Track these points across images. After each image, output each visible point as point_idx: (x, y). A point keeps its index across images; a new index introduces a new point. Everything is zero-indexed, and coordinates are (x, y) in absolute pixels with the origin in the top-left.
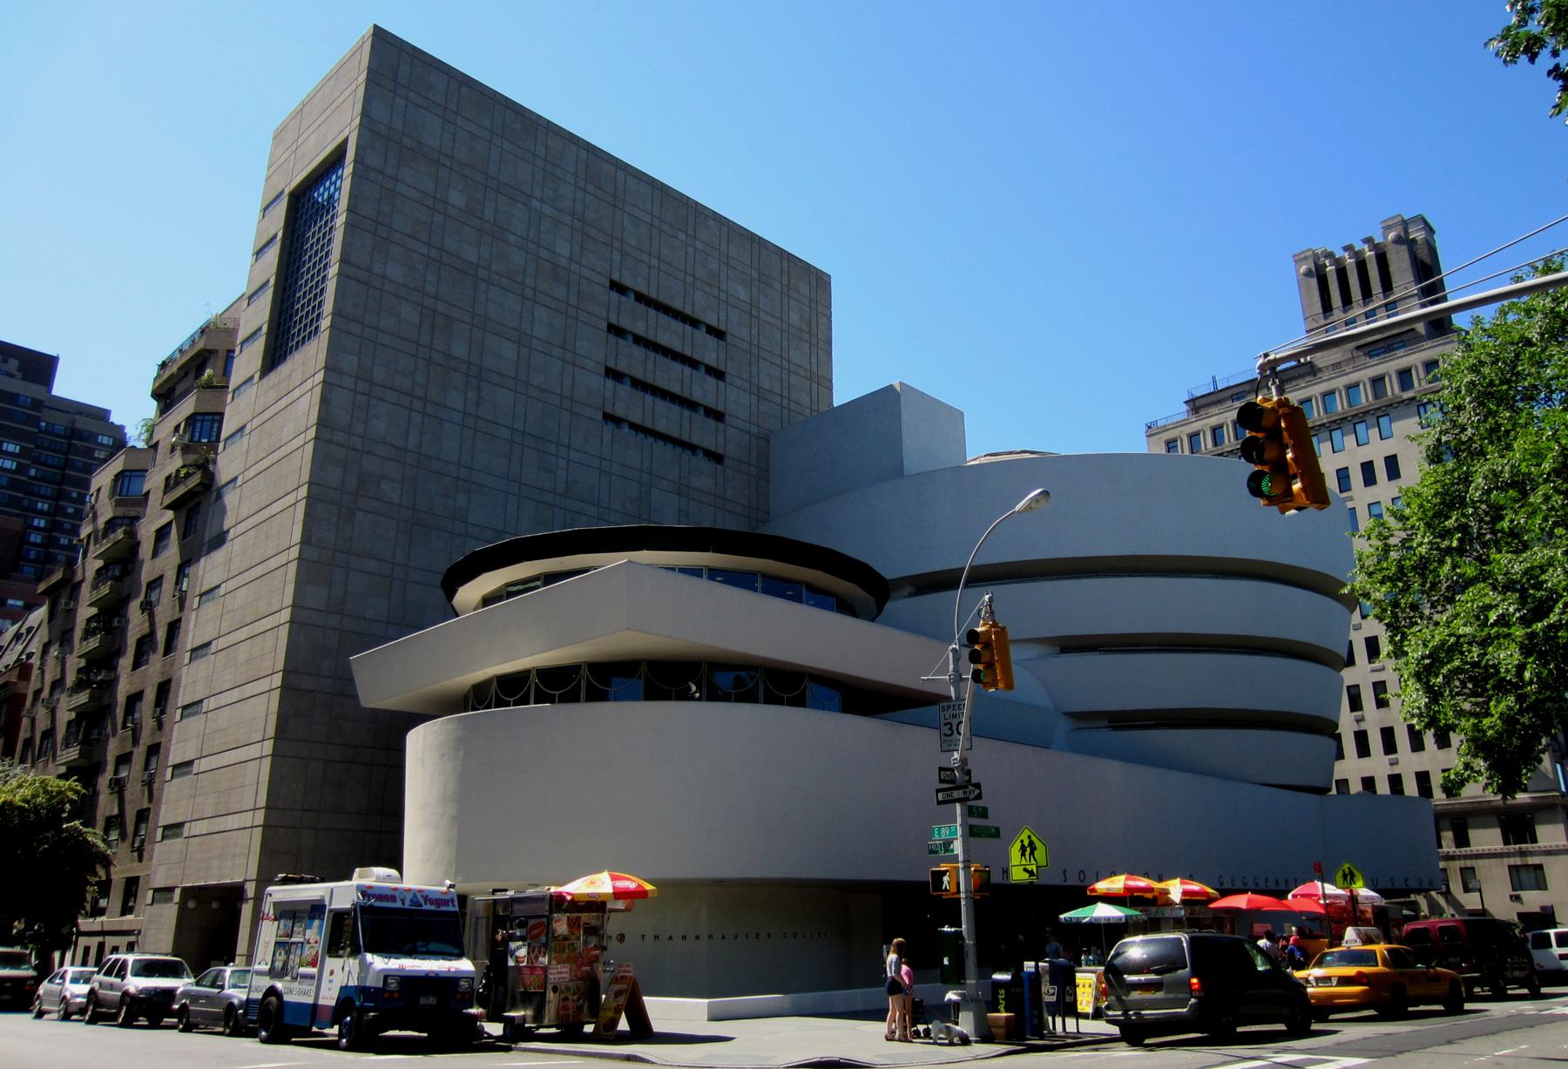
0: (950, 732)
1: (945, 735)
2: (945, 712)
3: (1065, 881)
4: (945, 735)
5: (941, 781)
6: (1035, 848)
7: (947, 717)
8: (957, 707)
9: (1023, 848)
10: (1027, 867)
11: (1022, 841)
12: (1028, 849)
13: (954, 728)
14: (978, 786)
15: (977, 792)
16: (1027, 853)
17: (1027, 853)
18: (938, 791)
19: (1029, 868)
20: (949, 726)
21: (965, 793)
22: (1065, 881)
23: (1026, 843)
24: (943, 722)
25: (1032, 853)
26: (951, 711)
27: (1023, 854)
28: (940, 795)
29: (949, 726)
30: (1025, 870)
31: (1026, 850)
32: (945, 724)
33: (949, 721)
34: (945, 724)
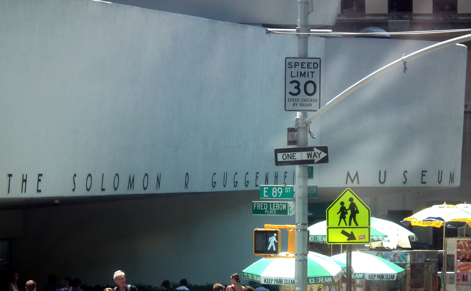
0: (296, 91)
1: (291, 93)
2: (293, 69)
3: (74, 190)
4: (291, 93)
5: (290, 143)
6: (357, 212)
7: (295, 74)
8: (305, 65)
9: (343, 212)
10: (347, 230)
11: (342, 203)
12: (349, 212)
13: (302, 87)
14: (324, 149)
15: (323, 155)
16: (348, 216)
17: (348, 216)
18: (277, 151)
19: (349, 231)
20: (296, 84)
21: (309, 155)
22: (74, 190)
23: (347, 205)
24: (289, 79)
25: (353, 216)
26: (299, 69)
27: (343, 217)
28: (280, 156)
29: (296, 84)
30: (344, 233)
31: (347, 213)
32: (292, 82)
33: (296, 79)
34: (292, 82)
